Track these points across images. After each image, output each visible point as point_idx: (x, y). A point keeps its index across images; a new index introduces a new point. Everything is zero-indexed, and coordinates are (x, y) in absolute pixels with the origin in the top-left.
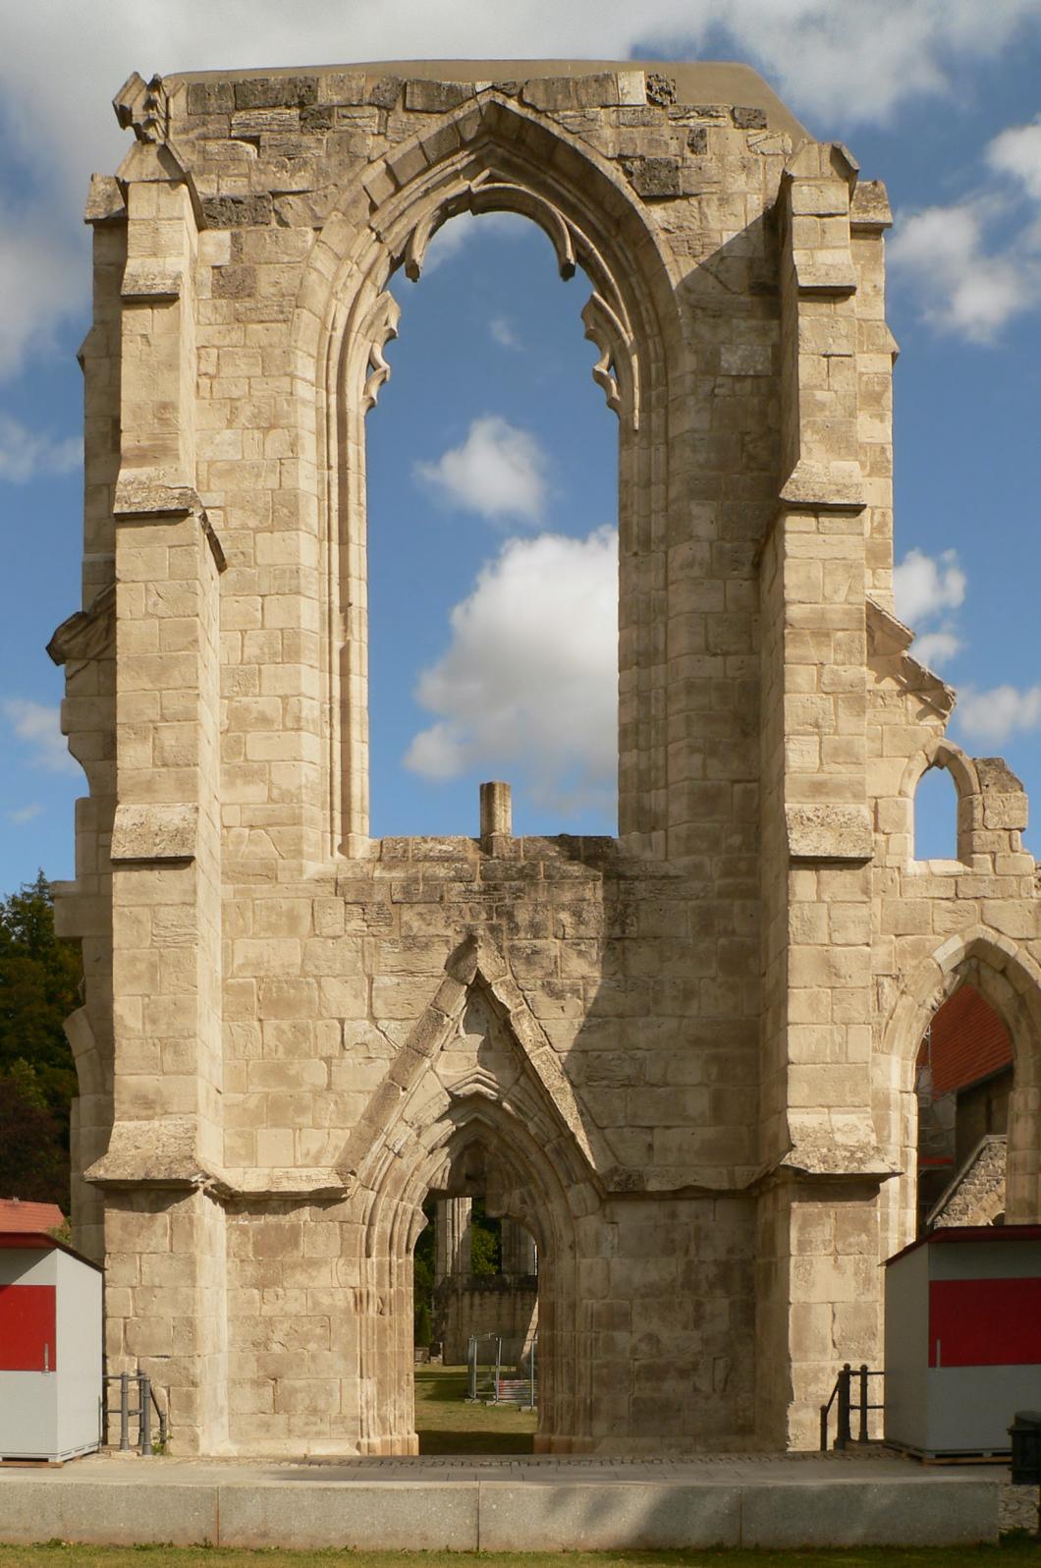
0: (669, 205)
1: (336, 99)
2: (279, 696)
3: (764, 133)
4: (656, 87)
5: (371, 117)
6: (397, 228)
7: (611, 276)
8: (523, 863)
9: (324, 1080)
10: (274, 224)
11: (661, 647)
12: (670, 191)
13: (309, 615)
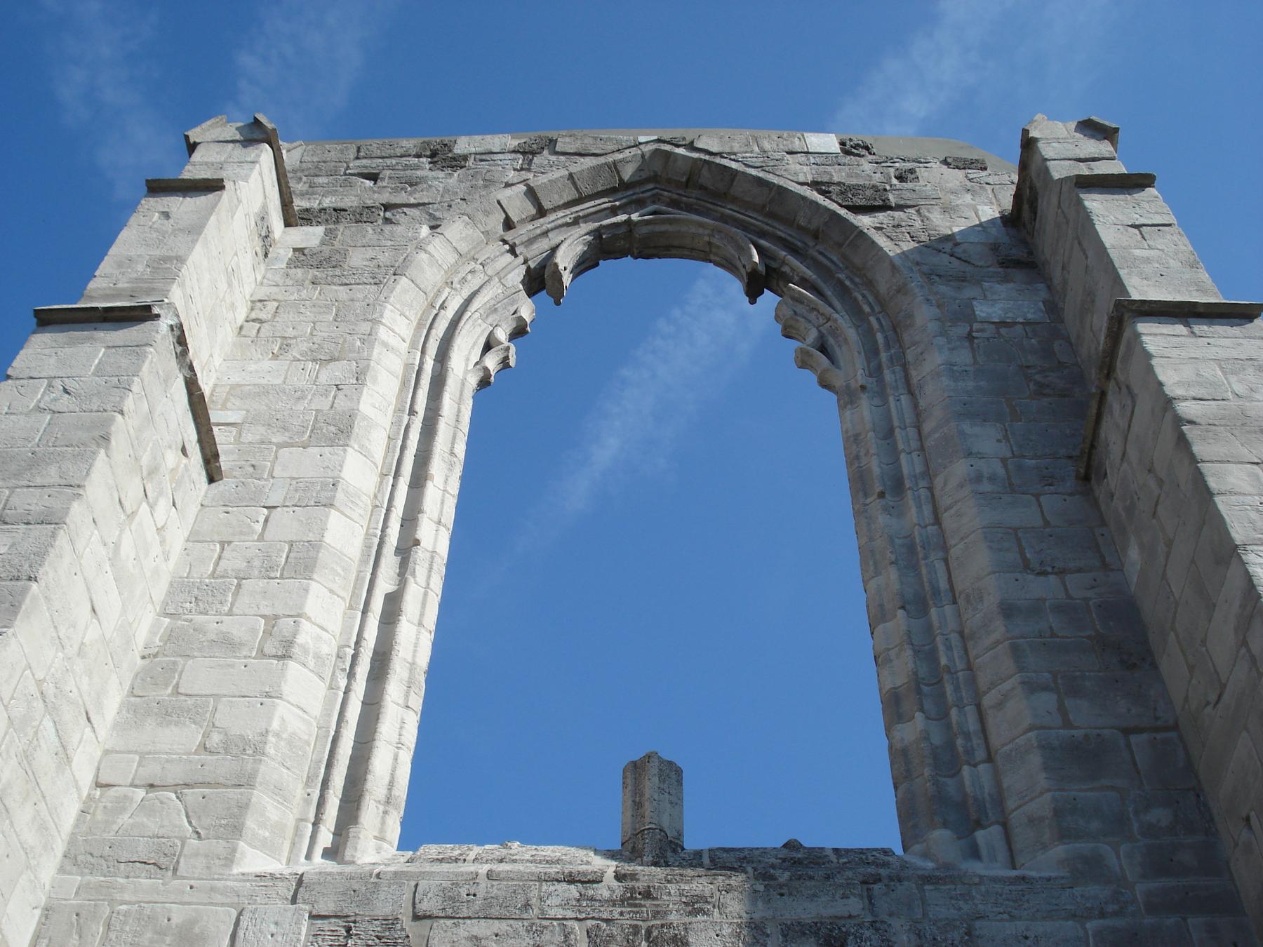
2: (261, 616)
3: (984, 173)
11: (943, 584)
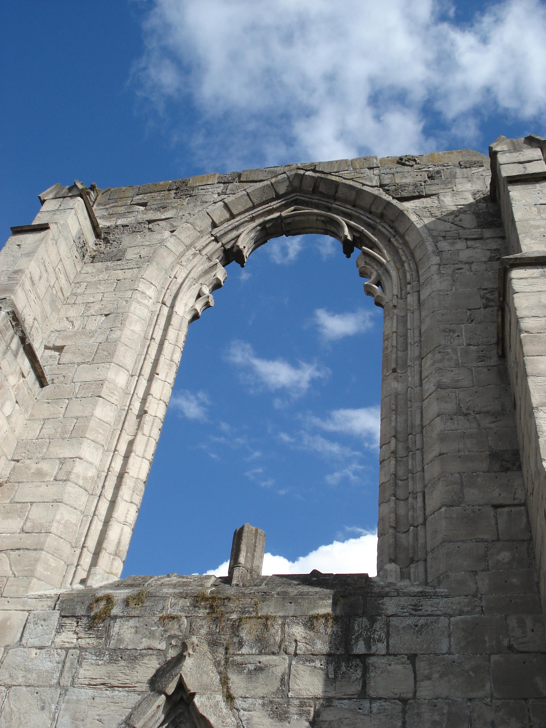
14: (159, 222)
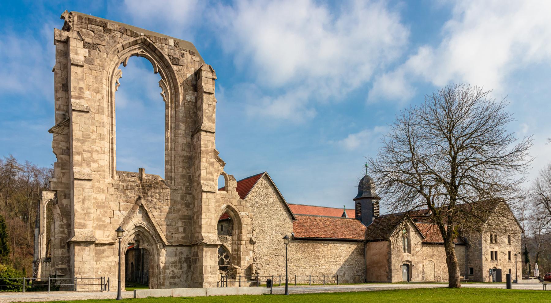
0: (177, 66)
1: (112, 28)
3: (195, 57)
4: (175, 43)
5: (119, 34)
6: (122, 57)
7: (165, 76)
8: (149, 184)
9: (110, 222)
10: (98, 51)
12: (178, 64)
13: (105, 131)
14: (101, 46)
